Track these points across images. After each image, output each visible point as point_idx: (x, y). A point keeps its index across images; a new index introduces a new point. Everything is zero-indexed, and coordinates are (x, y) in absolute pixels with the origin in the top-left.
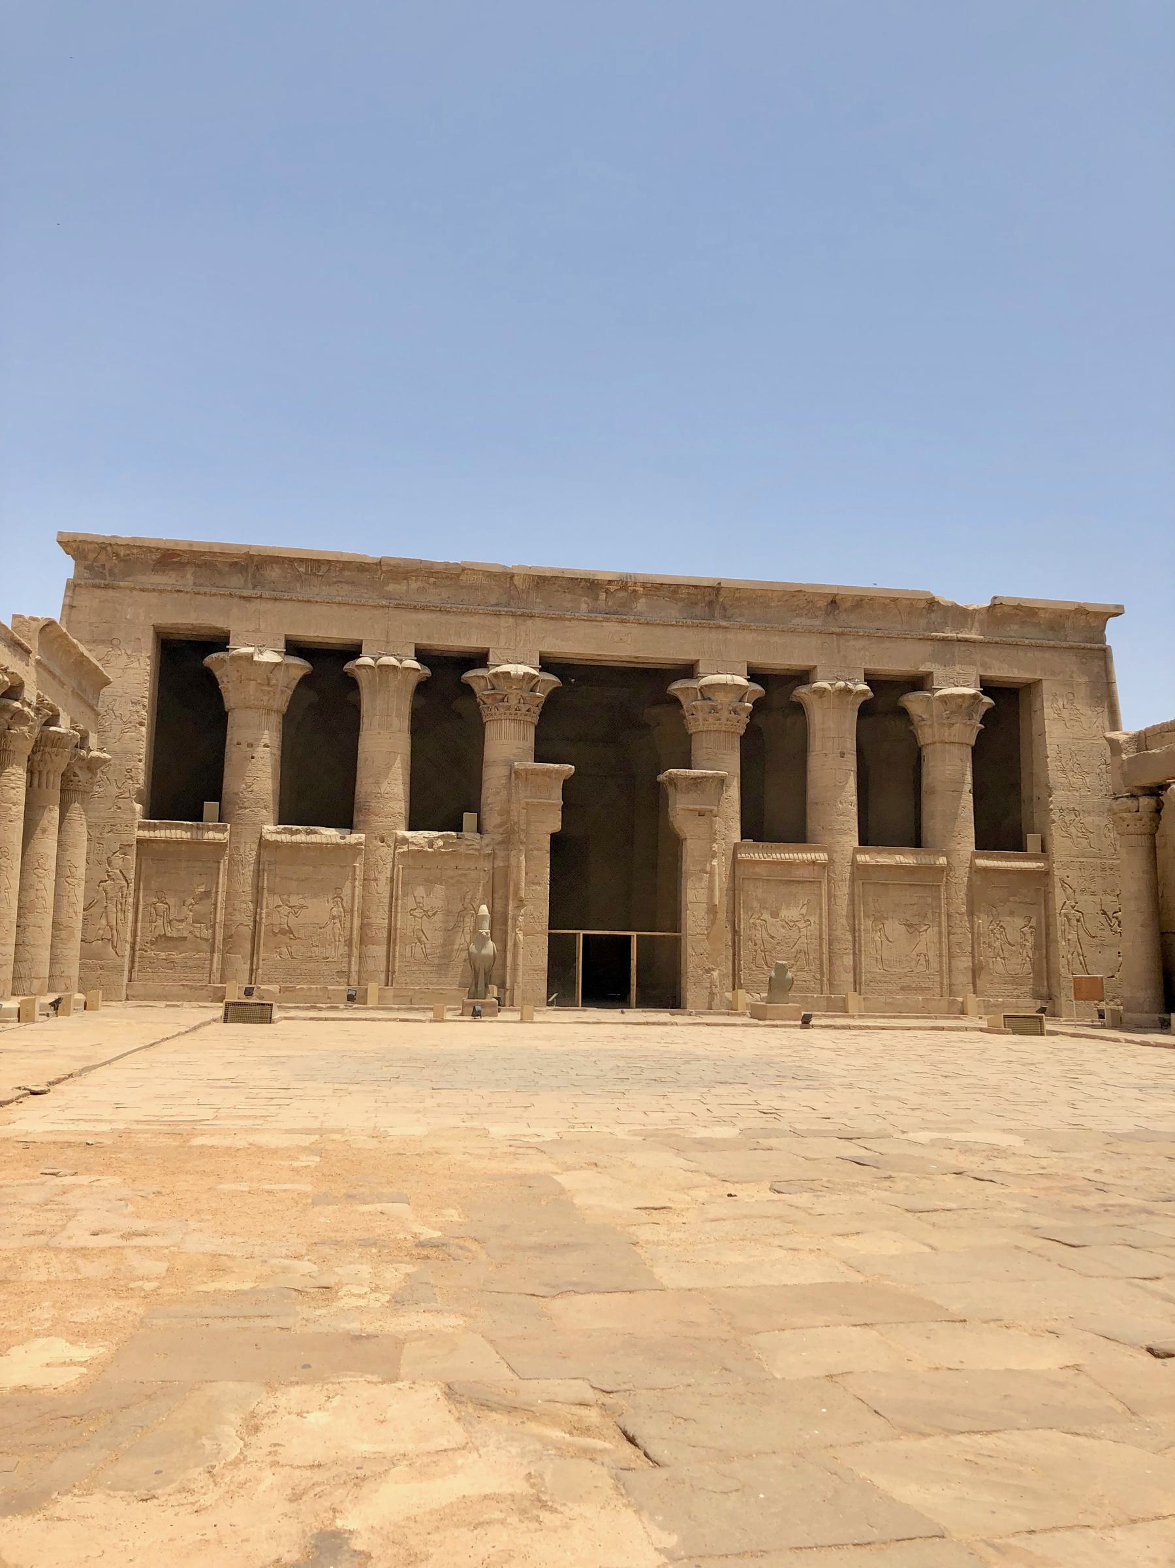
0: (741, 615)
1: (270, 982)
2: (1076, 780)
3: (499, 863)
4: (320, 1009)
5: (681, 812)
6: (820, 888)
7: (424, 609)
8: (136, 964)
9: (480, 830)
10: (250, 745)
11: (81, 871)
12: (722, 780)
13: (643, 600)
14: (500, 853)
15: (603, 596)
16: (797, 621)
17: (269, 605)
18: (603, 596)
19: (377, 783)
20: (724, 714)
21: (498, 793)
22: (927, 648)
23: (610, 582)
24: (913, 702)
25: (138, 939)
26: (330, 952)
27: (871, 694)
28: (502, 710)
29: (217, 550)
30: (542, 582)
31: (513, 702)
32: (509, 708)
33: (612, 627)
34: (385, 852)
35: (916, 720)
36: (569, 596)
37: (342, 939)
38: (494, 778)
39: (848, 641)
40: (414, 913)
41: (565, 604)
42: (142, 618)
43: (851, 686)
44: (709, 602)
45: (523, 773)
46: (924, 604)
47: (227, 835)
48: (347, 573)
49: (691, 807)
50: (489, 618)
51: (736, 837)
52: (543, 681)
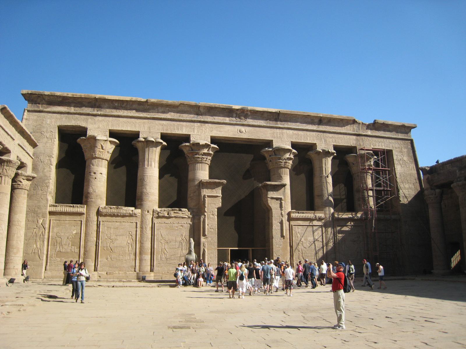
1: (102, 271)
2: (407, 186)
4: (124, 282)
8: (48, 263)
10: (95, 173)
11: (23, 223)
12: (284, 186)
17: (103, 118)
23: (237, 110)
24: (350, 158)
25: (49, 253)
26: (127, 257)
27: (335, 154)
29: (83, 97)
34: (149, 217)
37: (132, 253)
40: (161, 241)
42: (53, 123)
43: (330, 151)
47: (85, 210)
52: (213, 147)
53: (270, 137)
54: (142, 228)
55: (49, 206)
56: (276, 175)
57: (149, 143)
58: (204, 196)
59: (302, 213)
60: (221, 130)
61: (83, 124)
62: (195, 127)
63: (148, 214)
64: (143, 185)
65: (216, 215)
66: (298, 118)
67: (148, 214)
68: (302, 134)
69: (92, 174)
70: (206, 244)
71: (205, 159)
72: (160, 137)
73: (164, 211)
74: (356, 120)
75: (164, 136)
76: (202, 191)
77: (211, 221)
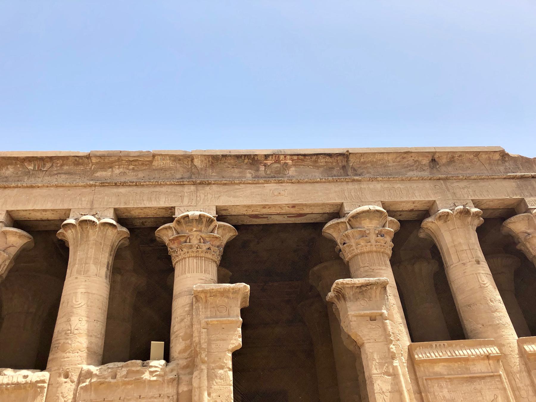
0: (368, 173)
3: (183, 388)
5: (354, 319)
6: (502, 382)
7: (123, 184)
9: (167, 357)
12: (384, 286)
13: (293, 169)
14: (185, 378)
15: (262, 168)
16: (410, 174)
18: (262, 168)
19: (69, 320)
20: (373, 237)
21: (182, 320)
22: (513, 184)
23: (266, 156)
28: (185, 250)
30: (216, 160)
31: (195, 242)
32: (191, 247)
33: (272, 187)
35: (522, 237)
36: (236, 170)
38: (180, 306)
39: (453, 183)
41: (234, 175)
44: (342, 165)
45: (202, 296)
46: (497, 157)
48: (66, 168)
49: (362, 313)
50: (175, 187)
51: (405, 340)
53: (337, 199)
56: (362, 269)
60: (238, 194)
62: (186, 194)
63: (66, 382)
65: (231, 366)
66: (388, 161)
67: (66, 382)
68: (402, 187)
72: (111, 213)
74: (507, 151)
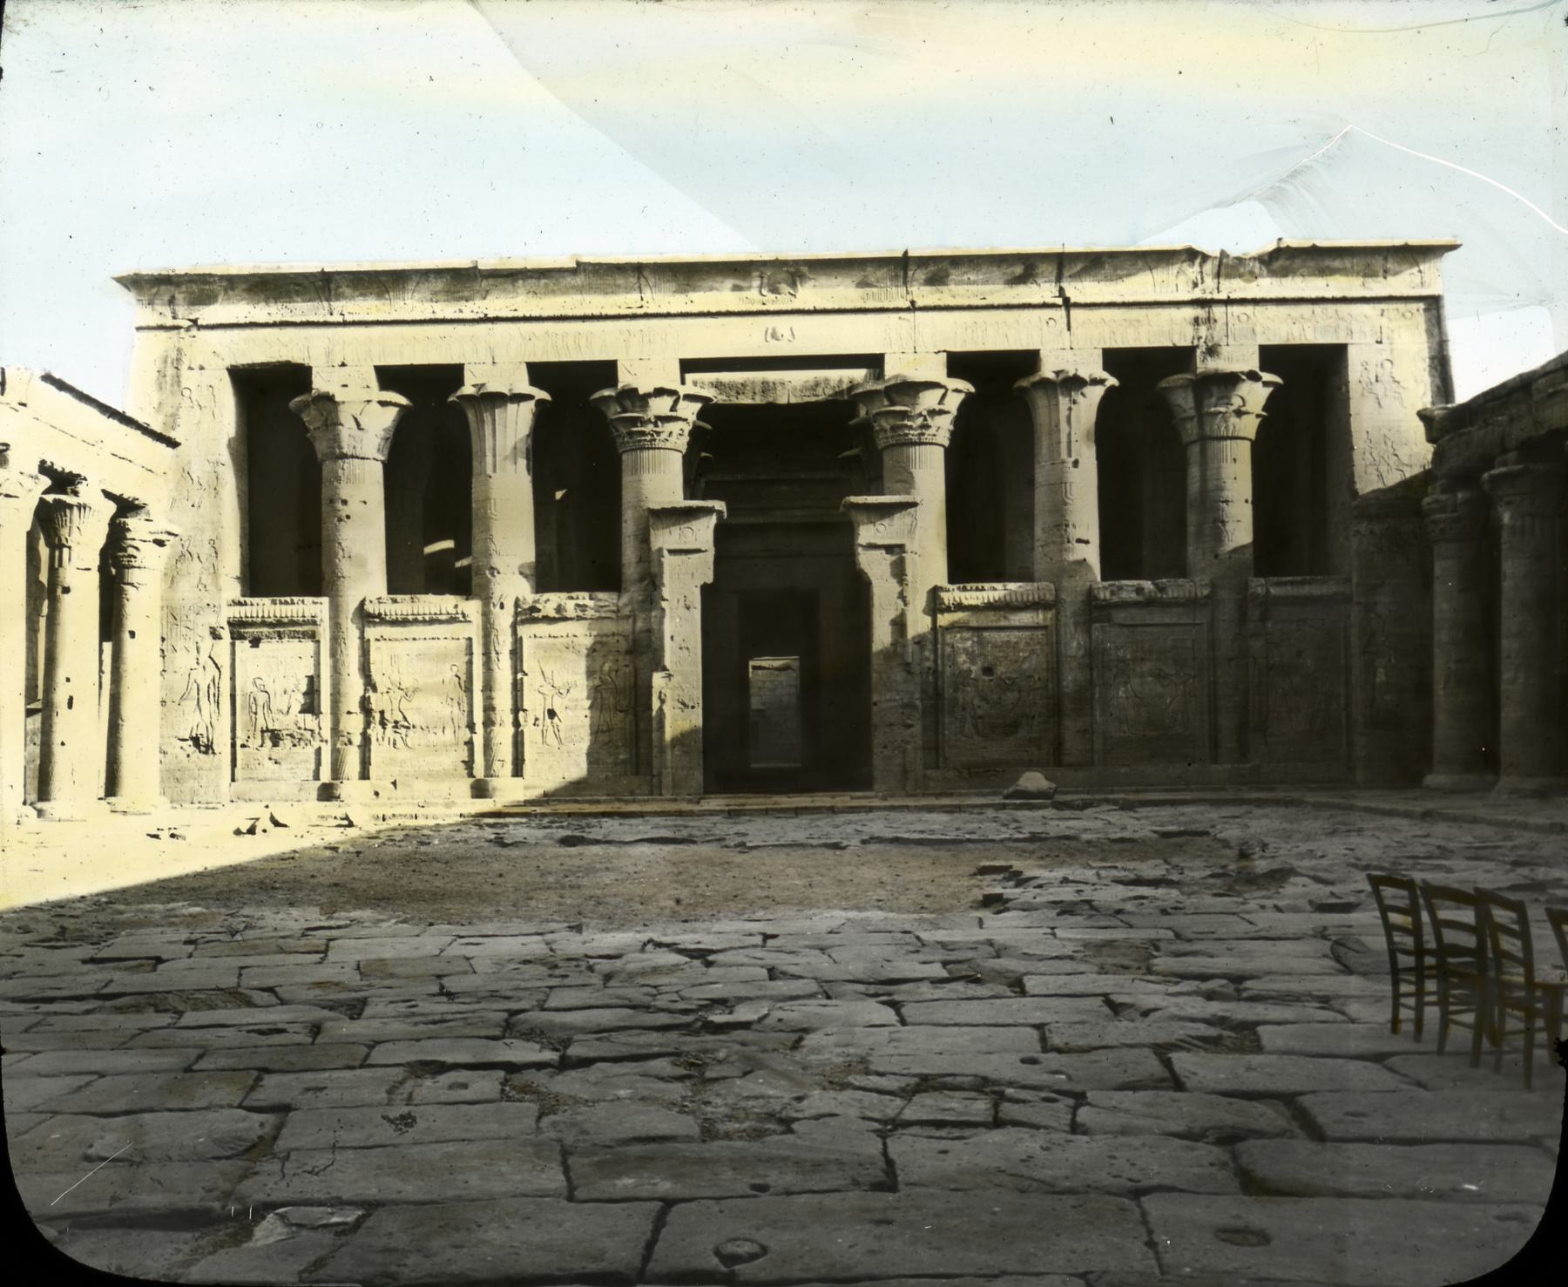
10: (345, 502)
27: (1112, 381)
34: (503, 619)
54: (487, 654)
55: (224, 605)
57: (494, 400)
58: (660, 550)
59: (977, 589)
61: (297, 357)
64: (487, 529)
69: (339, 505)
70: (668, 692)
71: (663, 436)
73: (551, 601)
75: (539, 373)
76: (652, 538)
77: (681, 630)
